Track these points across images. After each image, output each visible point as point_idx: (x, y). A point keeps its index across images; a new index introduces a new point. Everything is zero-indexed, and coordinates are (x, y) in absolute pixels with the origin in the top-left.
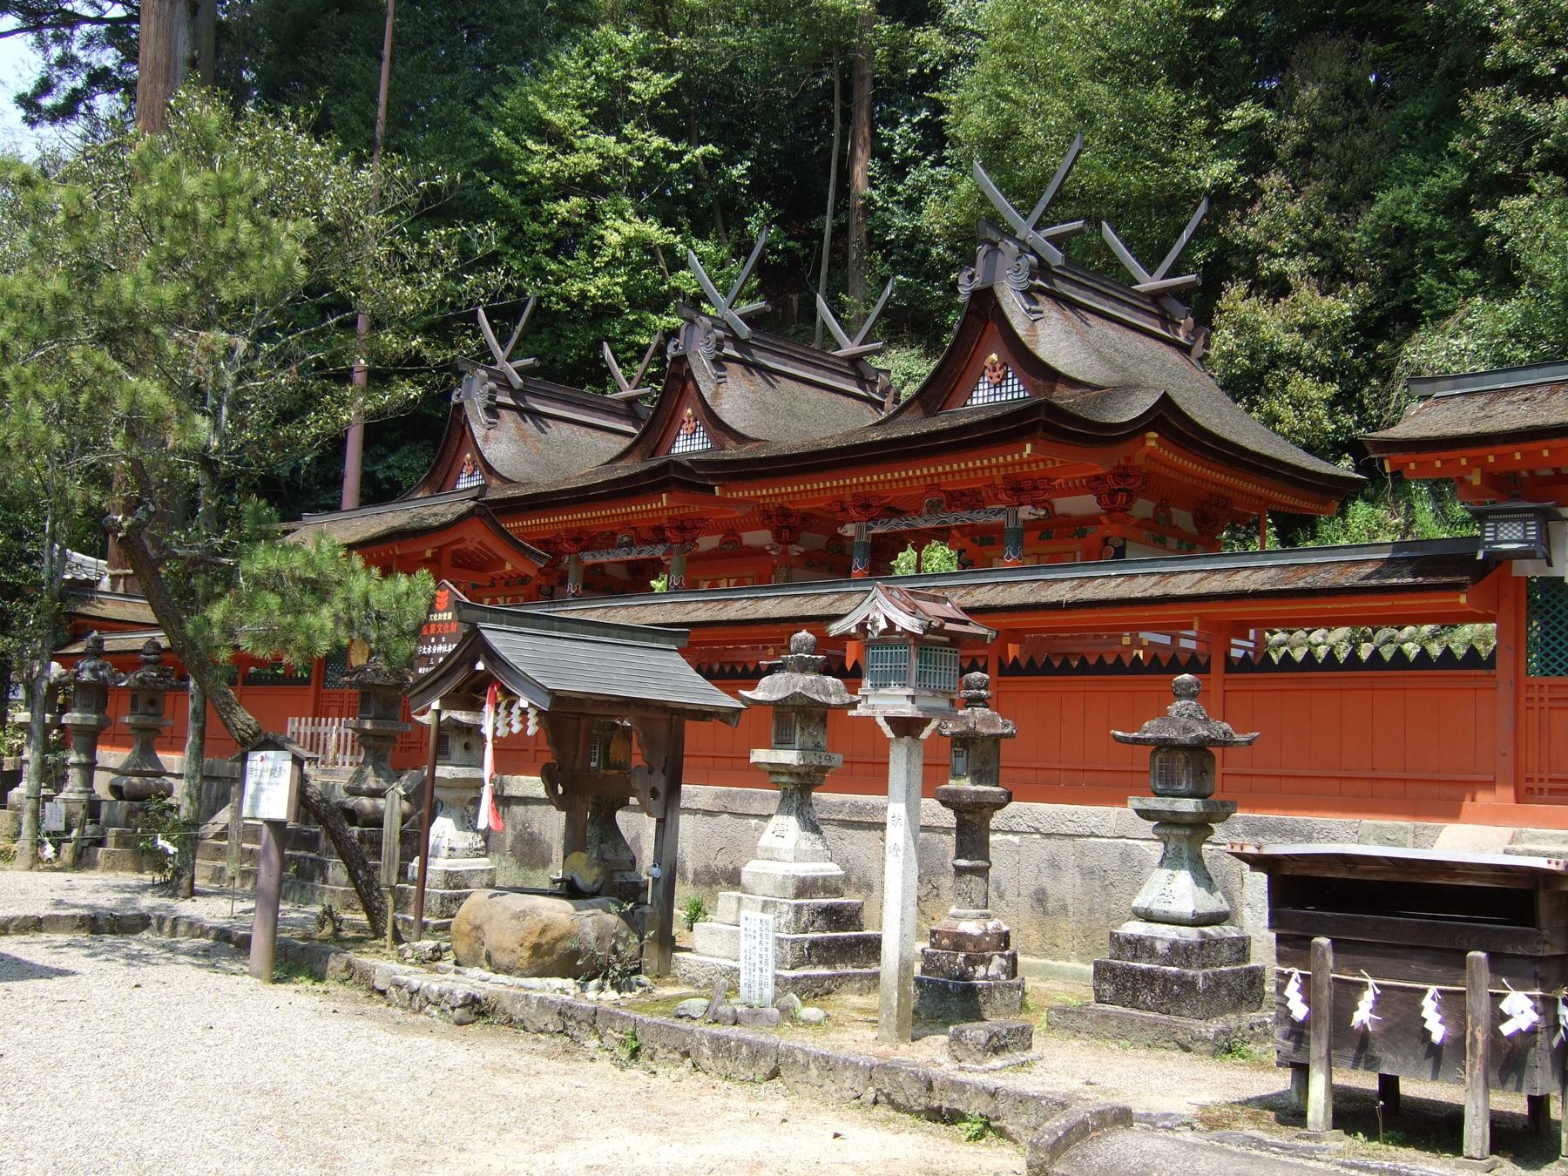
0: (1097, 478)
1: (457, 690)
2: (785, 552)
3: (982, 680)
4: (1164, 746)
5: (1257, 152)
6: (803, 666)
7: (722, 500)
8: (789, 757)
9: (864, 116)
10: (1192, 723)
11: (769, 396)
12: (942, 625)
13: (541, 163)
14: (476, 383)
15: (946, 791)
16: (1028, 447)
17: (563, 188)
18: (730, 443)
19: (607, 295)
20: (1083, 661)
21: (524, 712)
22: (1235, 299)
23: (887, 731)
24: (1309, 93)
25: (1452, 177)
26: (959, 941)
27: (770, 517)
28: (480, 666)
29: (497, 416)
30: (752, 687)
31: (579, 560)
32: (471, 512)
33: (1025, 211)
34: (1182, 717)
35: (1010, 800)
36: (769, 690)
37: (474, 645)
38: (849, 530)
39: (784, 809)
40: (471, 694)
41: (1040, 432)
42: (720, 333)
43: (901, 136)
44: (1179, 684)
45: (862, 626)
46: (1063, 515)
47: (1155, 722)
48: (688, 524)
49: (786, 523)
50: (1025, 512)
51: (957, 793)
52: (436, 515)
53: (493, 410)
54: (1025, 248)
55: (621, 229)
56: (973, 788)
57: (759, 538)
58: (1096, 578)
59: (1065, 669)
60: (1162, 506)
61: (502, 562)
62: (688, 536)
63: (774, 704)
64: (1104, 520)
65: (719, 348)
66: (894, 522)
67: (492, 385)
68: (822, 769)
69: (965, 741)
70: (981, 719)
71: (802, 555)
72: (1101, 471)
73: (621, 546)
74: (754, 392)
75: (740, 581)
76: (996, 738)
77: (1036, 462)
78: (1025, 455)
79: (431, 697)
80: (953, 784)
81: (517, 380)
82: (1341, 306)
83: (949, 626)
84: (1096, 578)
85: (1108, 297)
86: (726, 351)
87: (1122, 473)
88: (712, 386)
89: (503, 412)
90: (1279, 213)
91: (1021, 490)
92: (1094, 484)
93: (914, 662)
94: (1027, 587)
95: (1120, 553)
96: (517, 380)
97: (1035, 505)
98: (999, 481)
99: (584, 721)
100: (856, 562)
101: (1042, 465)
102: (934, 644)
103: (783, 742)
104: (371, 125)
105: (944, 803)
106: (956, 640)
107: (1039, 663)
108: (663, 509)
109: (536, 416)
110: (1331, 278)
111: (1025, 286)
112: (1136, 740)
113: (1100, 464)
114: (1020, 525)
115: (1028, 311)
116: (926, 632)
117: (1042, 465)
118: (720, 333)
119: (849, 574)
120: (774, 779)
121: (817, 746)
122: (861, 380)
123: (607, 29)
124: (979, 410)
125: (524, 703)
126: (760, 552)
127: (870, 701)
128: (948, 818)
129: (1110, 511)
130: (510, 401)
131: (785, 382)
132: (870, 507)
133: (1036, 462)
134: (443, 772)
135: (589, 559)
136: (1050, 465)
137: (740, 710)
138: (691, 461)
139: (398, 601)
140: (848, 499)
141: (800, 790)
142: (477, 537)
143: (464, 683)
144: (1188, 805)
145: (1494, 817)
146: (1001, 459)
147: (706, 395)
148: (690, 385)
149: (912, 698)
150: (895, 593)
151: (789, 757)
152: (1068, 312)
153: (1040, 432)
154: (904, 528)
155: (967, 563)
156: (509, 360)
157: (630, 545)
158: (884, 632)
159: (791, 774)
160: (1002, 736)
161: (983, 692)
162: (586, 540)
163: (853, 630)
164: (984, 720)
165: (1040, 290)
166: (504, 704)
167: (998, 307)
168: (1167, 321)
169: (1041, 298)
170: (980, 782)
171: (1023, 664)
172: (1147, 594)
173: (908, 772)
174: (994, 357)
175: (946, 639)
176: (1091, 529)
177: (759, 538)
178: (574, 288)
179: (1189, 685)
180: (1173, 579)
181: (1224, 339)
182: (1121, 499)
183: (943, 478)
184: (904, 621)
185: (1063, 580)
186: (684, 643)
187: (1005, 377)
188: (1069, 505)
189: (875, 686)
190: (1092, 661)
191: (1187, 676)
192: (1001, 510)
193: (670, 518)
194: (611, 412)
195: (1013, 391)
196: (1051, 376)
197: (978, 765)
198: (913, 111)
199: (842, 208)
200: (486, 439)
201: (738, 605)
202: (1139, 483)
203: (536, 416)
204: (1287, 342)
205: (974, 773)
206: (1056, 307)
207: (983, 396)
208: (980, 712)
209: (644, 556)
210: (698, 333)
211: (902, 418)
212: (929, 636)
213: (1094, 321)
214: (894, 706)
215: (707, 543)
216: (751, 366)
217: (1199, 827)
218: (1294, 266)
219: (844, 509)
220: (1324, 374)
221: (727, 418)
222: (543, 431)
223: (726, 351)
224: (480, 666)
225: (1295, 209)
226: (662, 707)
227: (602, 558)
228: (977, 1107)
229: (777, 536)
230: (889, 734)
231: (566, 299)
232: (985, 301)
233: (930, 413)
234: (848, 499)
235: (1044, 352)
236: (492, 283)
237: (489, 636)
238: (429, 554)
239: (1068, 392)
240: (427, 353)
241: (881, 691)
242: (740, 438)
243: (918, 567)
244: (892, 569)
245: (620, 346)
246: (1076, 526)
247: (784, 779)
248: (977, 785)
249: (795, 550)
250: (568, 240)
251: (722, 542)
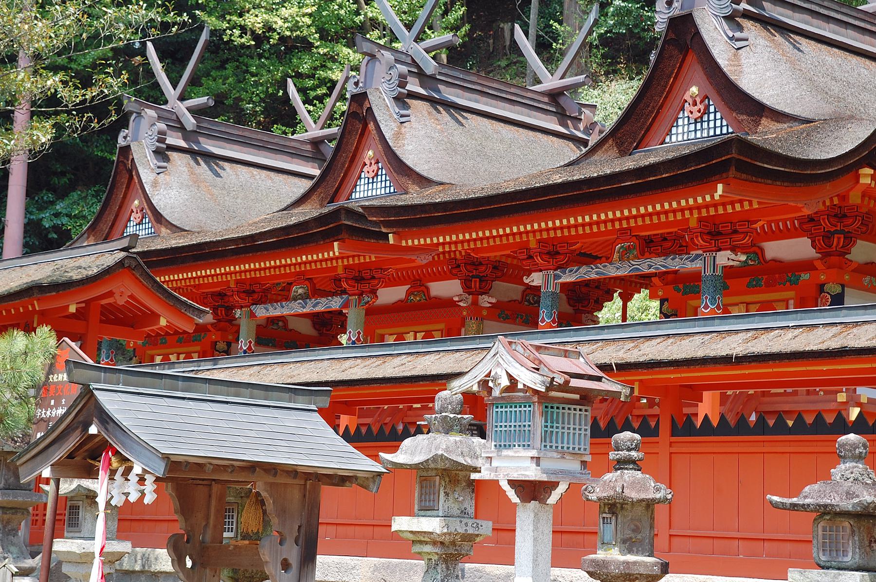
0: (811, 219)
1: (71, 456)
2: (475, 303)
3: (632, 440)
4: (826, 513)
6: (448, 428)
7: (396, 248)
8: (432, 525)
10: (857, 488)
12: (567, 382)
14: (144, 123)
15: (593, 561)
16: (720, 187)
18: (413, 188)
19: (296, 27)
20: (799, 420)
21: (142, 480)
23: (511, 494)
27: (458, 266)
28: (93, 430)
29: (167, 159)
30: (394, 449)
31: (252, 315)
32: (120, 264)
35: (665, 569)
36: (412, 451)
37: (88, 407)
38: (536, 279)
40: (88, 457)
41: (732, 172)
42: (404, 69)
44: (843, 445)
45: (484, 383)
46: (774, 260)
47: (816, 487)
48: (366, 274)
49: (477, 272)
50: (724, 258)
51: (604, 564)
52: (80, 267)
53: (162, 153)
56: (622, 558)
57: (447, 288)
58: (772, 329)
59: (781, 428)
61: (158, 317)
62: (367, 287)
63: (416, 467)
64: (818, 264)
65: (402, 85)
66: (584, 269)
67: (162, 126)
68: (469, 538)
69: (613, 507)
70: (636, 485)
71: (494, 306)
72: (807, 212)
73: (295, 299)
74: (441, 132)
75: (428, 334)
76: (649, 504)
77: (732, 203)
78: (717, 197)
79: (42, 464)
80: (600, 555)
81: (190, 122)
83: (575, 383)
84: (772, 329)
85: (828, 19)
86: (409, 87)
87: (839, 213)
88: (394, 126)
89: (173, 155)
91: (719, 234)
92: (807, 226)
93: (539, 421)
94: (698, 339)
95: (838, 300)
96: (190, 122)
97: (734, 249)
98: (693, 223)
99: (216, 488)
100: (543, 313)
101: (738, 207)
102: (553, 399)
103: (427, 509)
105: (591, 574)
106: (586, 397)
107: (731, 420)
108: (337, 258)
109: (210, 157)
111: (728, 11)
112: (794, 506)
113: (812, 203)
114: (719, 272)
115: (732, 39)
116: (548, 389)
117: (738, 207)
118: (404, 69)
119: (535, 325)
120: (416, 549)
121: (464, 513)
122: (563, 116)
124: (677, 147)
125: (137, 469)
126: (448, 303)
127: (495, 464)
129: (825, 255)
130: (182, 144)
131: (474, 121)
132: (557, 254)
133: (732, 203)
134: (59, 545)
135: (262, 312)
136: (747, 206)
137: (380, 474)
138: (363, 207)
139: (13, 360)
140: (533, 244)
141: (446, 561)
142: (125, 291)
143: (77, 449)
146: (691, 201)
147: (388, 135)
148: (371, 126)
149: (537, 460)
150: (519, 348)
151: (432, 525)
152: (778, 38)
153: (732, 172)
154: (594, 276)
155: (672, 311)
156: (182, 98)
157: (305, 297)
158: (507, 389)
159: (434, 543)
160: (653, 500)
161: (634, 454)
162: (258, 292)
163: (475, 388)
164: (633, 484)
165: (746, 15)
166: (121, 470)
167: (697, 34)
169: (746, 23)
170: (630, 551)
171: (715, 422)
172: (823, 347)
173: (535, 539)
174: (694, 90)
175: (577, 397)
176: (805, 276)
177: (447, 288)
179: (855, 446)
180: (855, 330)
182: (837, 241)
183: (632, 223)
184: (527, 378)
185: (737, 332)
186: (325, 402)
187: (707, 111)
188: (779, 250)
189: (499, 447)
190: (809, 419)
191: (852, 437)
192: (698, 256)
193: (346, 268)
194: (295, 154)
195: (717, 126)
196: (750, 108)
197: (628, 533)
200: (155, 184)
201: (397, 361)
202: (857, 224)
203: (210, 157)
205: (624, 541)
206: (764, 33)
208: (630, 475)
209: (320, 308)
210: (380, 69)
211: (596, 157)
212: (553, 394)
213: (804, 43)
214: (517, 469)
215: (389, 295)
216: (435, 102)
219: (530, 257)
221: (410, 160)
222: (218, 175)
223: (409, 87)
224: (93, 430)
226: (292, 471)
227: (275, 311)
229: (467, 287)
230: (515, 499)
233: (624, 152)
234: (533, 244)
235: (748, 83)
236: (132, 18)
237: (101, 396)
238: (72, 309)
239: (774, 126)
240: (64, 93)
241: (505, 452)
242: (423, 181)
243: (624, 318)
244: (596, 321)
245: (310, 83)
246: (780, 274)
247: (428, 548)
249: (486, 301)
251: (409, 293)
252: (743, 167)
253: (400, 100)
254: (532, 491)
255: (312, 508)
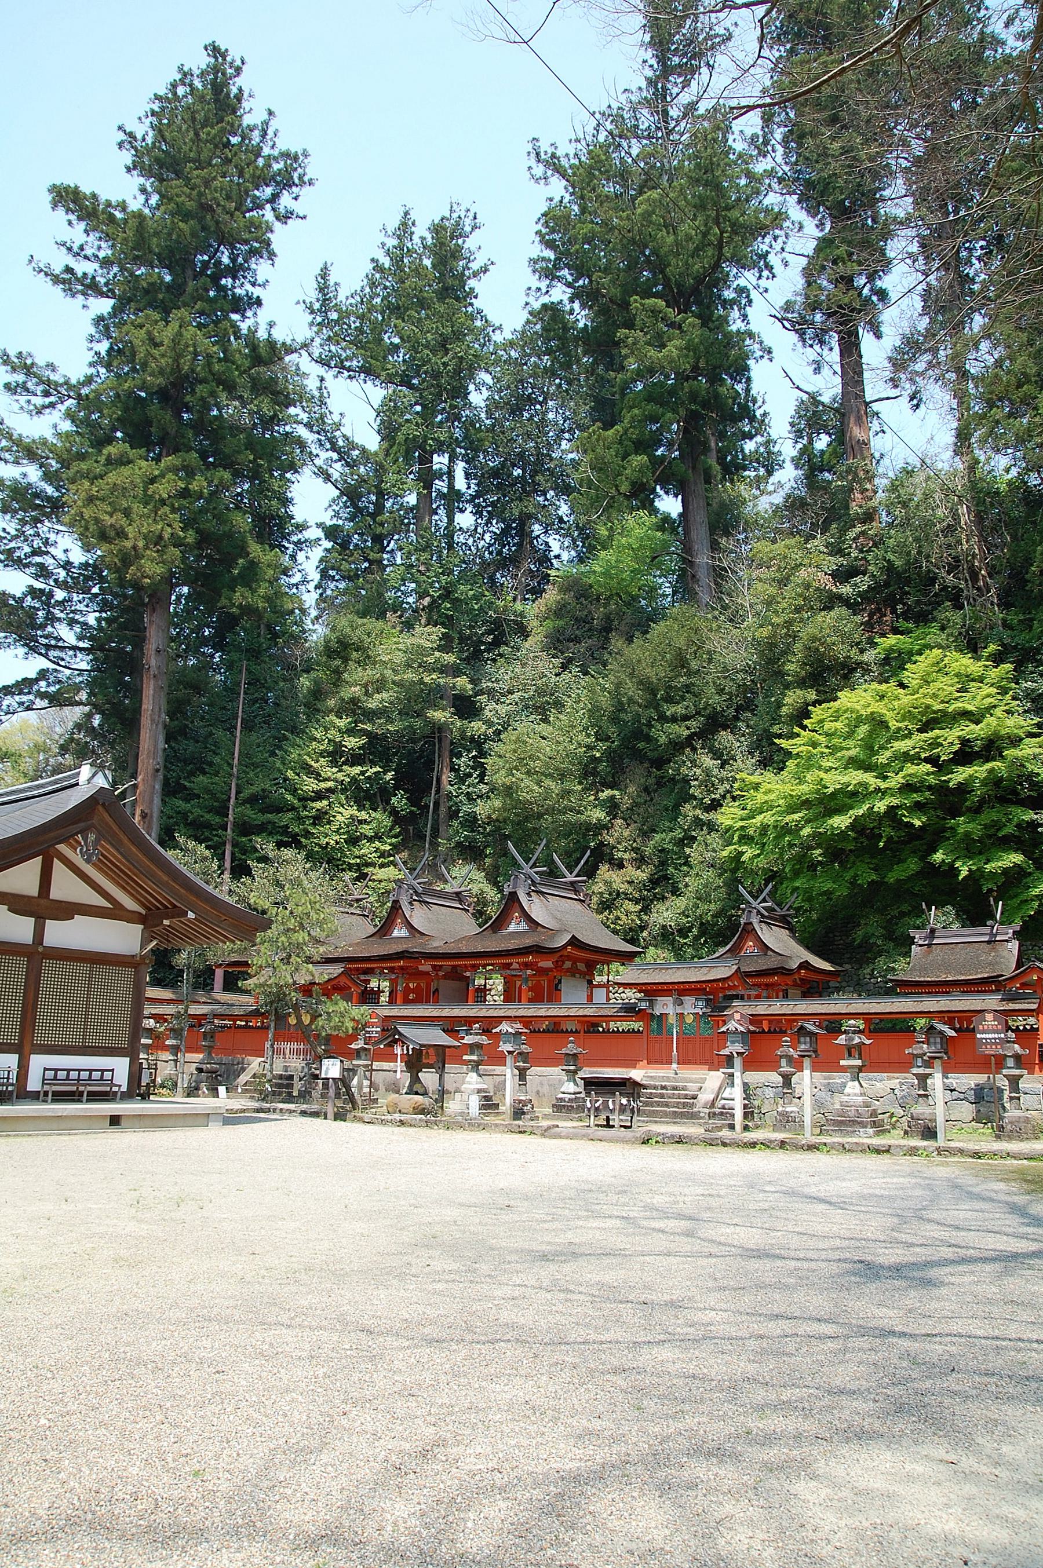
5: (612, 807)
6: (477, 1034)
9: (447, 754)
11: (430, 914)
13: (310, 785)
17: (319, 796)
19: (337, 843)
22: (604, 870)
24: (631, 789)
25: (678, 834)
26: (520, 1101)
33: (527, 861)
34: (571, 1048)
39: (472, 1070)
43: (463, 762)
54: (528, 877)
55: (344, 813)
60: (574, 963)
82: (641, 875)
90: (620, 835)
103: (472, 1054)
104: (231, 766)
110: (640, 861)
122: (460, 901)
123: (332, 717)
126: (427, 973)
128: (517, 1072)
142: (343, 981)
144: (572, 1068)
145: (642, 1068)
151: (475, 1058)
168: (576, 892)
178: (324, 841)
181: (599, 887)
184: (510, 1030)
198: (469, 751)
199: (438, 791)
204: (624, 887)
207: (512, 927)
217: (575, 1072)
218: (626, 856)
220: (637, 902)
225: (626, 833)
228: (529, 1130)
231: (320, 846)
232: (513, 897)
248: (525, 1062)
249: (441, 973)
250: (320, 818)
252: (538, 952)
253: (411, 903)
254: (509, 1052)
255: (444, 1053)
